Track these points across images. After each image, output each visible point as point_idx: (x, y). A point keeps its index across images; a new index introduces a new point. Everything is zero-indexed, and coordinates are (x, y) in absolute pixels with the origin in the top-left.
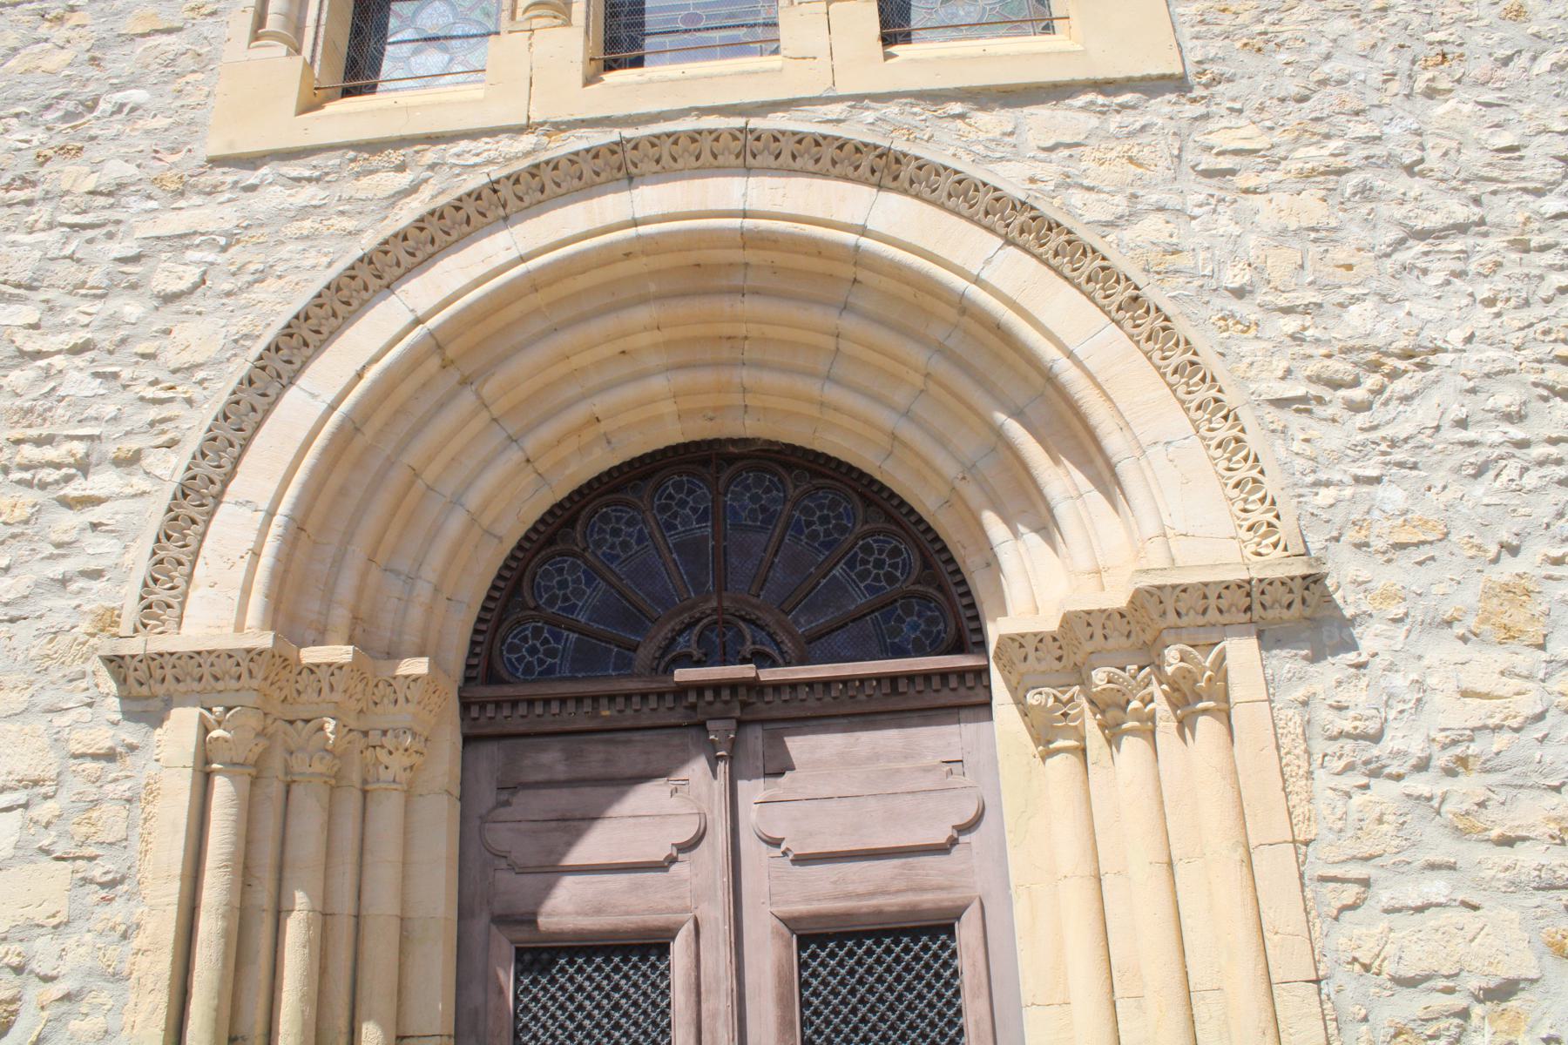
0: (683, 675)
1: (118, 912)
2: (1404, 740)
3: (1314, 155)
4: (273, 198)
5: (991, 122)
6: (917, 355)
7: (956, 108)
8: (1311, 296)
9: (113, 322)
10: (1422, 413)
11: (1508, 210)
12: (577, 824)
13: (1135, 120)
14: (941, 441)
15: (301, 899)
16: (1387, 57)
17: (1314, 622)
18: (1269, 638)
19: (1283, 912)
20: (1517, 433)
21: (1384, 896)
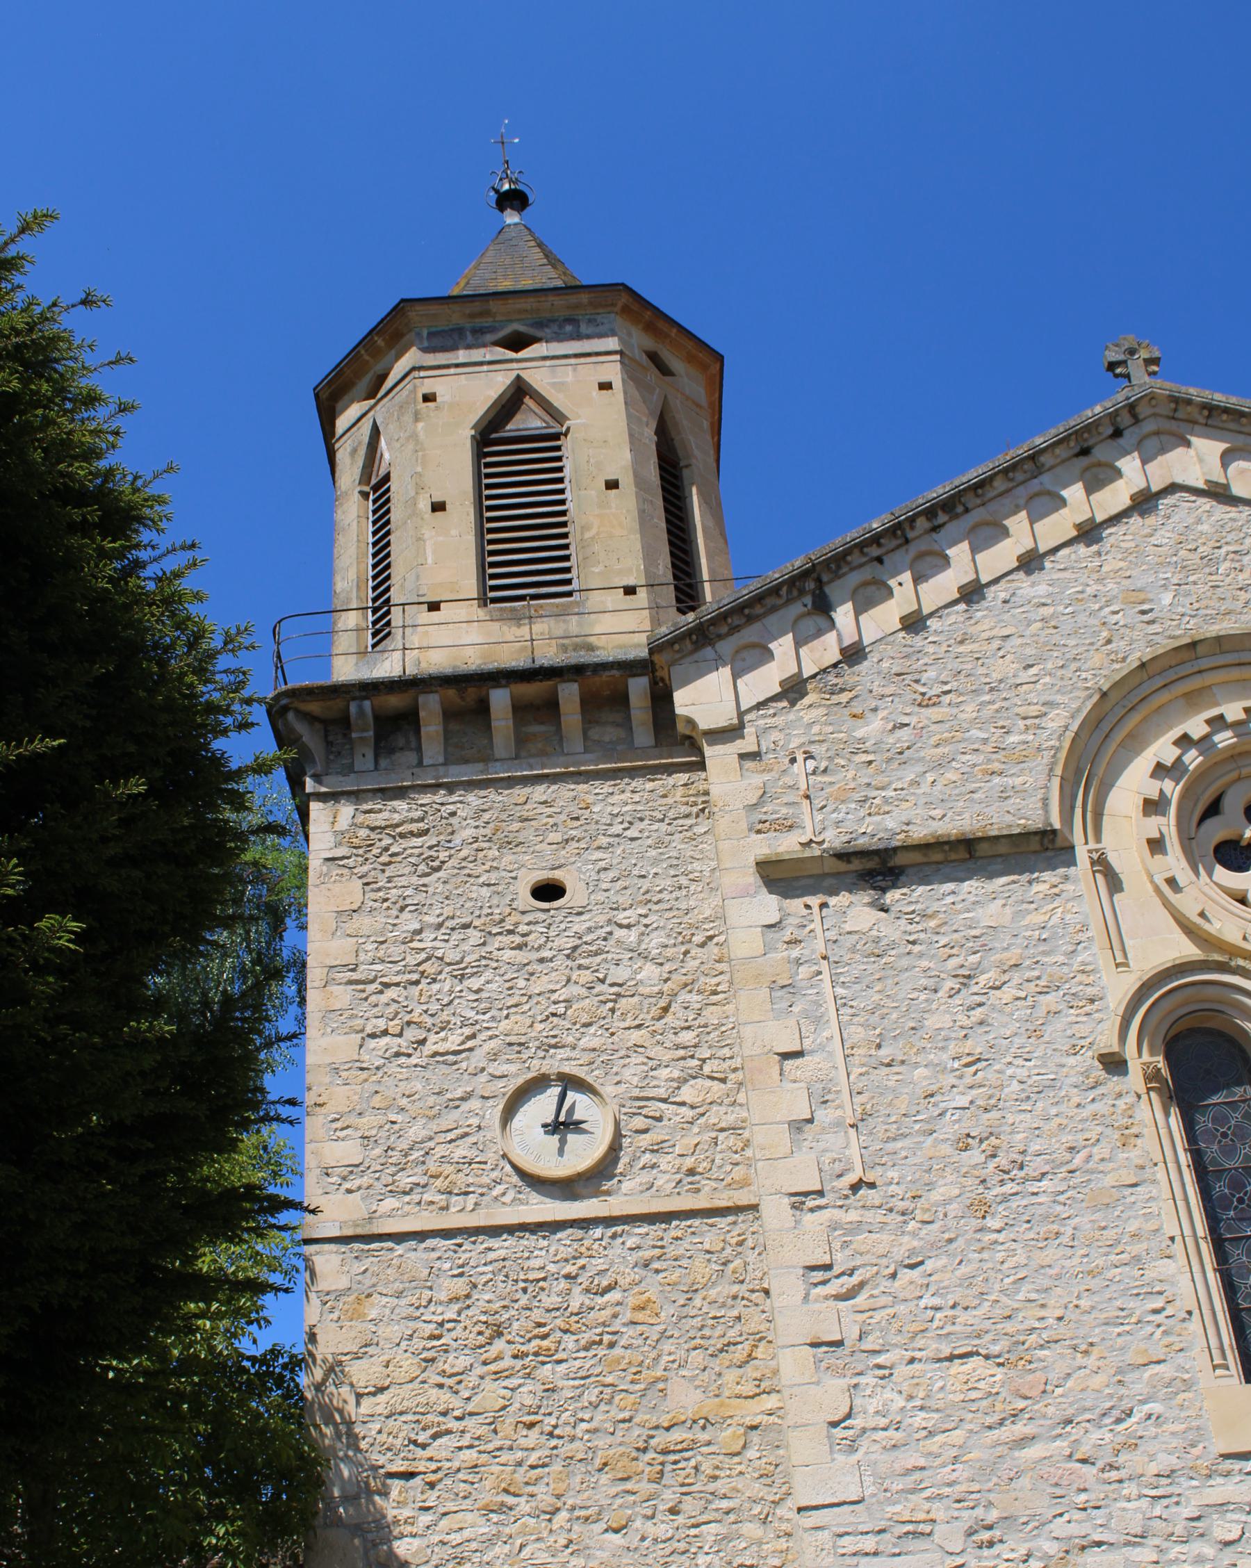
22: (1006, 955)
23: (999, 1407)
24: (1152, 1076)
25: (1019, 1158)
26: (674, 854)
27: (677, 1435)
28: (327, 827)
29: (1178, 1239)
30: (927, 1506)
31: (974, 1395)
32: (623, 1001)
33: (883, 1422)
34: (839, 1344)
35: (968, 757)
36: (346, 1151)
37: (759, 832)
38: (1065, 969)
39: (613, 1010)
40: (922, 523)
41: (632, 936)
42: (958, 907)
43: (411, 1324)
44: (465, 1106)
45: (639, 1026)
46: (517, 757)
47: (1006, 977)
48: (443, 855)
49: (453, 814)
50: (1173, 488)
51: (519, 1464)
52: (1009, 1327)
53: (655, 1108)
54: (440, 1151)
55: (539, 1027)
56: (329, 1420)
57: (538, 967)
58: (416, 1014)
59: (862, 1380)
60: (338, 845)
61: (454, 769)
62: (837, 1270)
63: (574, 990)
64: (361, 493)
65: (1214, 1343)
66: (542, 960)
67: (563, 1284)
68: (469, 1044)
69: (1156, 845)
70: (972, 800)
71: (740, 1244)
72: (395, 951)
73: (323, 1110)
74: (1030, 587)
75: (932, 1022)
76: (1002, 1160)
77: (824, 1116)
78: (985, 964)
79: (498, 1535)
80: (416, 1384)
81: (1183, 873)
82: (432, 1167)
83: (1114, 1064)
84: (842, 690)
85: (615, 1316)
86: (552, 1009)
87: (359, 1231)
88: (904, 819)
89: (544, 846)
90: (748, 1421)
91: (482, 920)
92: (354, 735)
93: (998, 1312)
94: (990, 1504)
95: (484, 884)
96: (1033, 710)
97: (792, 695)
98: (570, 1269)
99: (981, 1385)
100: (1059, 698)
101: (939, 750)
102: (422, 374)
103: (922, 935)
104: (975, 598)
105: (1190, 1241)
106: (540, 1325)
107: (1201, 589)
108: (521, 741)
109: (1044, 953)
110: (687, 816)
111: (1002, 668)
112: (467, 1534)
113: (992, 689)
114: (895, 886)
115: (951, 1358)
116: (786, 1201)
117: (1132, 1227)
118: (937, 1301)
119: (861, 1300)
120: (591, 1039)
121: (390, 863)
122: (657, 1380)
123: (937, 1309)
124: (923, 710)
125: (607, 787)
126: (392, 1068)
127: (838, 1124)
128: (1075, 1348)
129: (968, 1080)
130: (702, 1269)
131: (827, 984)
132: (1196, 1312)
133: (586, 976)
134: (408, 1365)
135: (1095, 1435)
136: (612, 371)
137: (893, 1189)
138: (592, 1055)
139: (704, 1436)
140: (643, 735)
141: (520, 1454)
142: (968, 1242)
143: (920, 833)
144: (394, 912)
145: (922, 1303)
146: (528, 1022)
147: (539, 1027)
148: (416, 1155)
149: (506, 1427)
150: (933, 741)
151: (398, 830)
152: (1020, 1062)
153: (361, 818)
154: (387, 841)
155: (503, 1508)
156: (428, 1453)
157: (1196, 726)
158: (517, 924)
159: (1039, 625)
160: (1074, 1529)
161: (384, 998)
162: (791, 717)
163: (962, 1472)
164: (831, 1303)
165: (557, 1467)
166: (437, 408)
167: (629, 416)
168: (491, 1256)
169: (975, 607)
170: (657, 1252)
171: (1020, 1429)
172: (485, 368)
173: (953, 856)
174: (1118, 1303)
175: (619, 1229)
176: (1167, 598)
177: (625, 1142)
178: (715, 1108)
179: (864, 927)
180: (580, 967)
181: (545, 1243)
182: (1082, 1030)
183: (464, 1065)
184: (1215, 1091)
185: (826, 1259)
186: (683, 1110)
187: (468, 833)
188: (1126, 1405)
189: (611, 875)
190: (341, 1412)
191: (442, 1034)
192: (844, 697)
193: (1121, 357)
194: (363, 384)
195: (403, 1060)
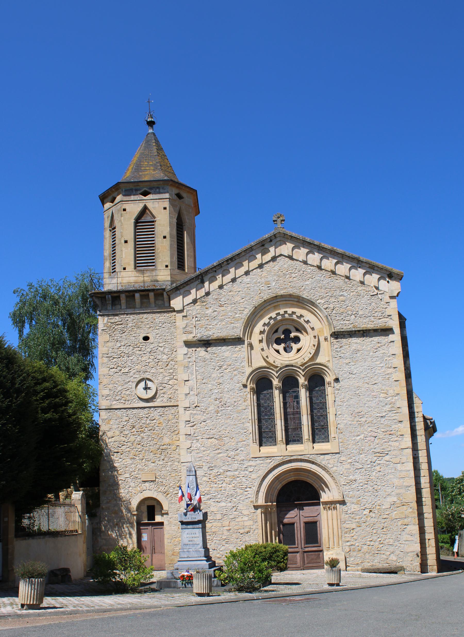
0: (295, 502)
1: (257, 524)
2: (349, 512)
3: (349, 461)
4: (258, 462)
5: (322, 456)
6: (315, 478)
7: (319, 455)
8: (347, 475)
9: (246, 474)
10: (354, 486)
11: (365, 467)
12: (286, 514)
13: (335, 457)
14: (317, 484)
15: (268, 522)
16: (358, 450)
17: (344, 503)
18: (340, 504)
19: (339, 524)
20: (362, 487)
21: (346, 523)
22: (229, 363)
23: (216, 447)
24: (252, 389)
25: (225, 403)
26: (171, 331)
27: (164, 447)
28: (102, 322)
29: (251, 420)
30: (202, 463)
31: (212, 445)
32: (159, 363)
33: (196, 449)
34: (190, 435)
35: (227, 319)
36: (106, 392)
37: (185, 334)
38: (239, 366)
39: (157, 365)
40: (225, 263)
42: (221, 352)
43: (118, 425)
44: (129, 384)
45: (162, 368)
46: (141, 308)
47: (228, 367)
48: (125, 330)
50: (281, 255)
51: (137, 451)
52: (219, 433)
53: (164, 385)
54: (124, 392)
55: (143, 368)
56: (103, 442)
58: (119, 364)
59: (194, 441)
60: (104, 326)
61: (128, 310)
62: (191, 422)
63: (151, 360)
64: (110, 230)
65: (254, 438)
66: (144, 354)
67: (146, 419)
68: (130, 371)
69: (261, 341)
70: (227, 329)
72: (116, 350)
73: (102, 383)
74: (246, 279)
75: (213, 376)
76: (222, 403)
77: (192, 393)
78: (224, 364)
79: (133, 463)
80: (119, 436)
82: (122, 396)
83: (245, 386)
84: (205, 302)
85: (155, 425)
86: (146, 364)
87: (109, 408)
88: (213, 332)
89: (145, 328)
90: (177, 445)
92: (107, 302)
93: (218, 431)
94: (212, 463)
96: (242, 309)
97: (194, 303)
98: (147, 416)
99: (213, 443)
100: (247, 307)
102: (123, 203)
103: (213, 358)
104: (234, 281)
105: (253, 420)
106: (141, 426)
107: (282, 282)
108: (142, 303)
111: (237, 299)
112: (128, 463)
113: (234, 304)
114: (210, 347)
115: (209, 438)
116: (183, 409)
117: (243, 417)
118: (208, 428)
119: (194, 427)
120: (153, 370)
121: (115, 331)
122: (162, 437)
123: (208, 430)
124: (220, 308)
125: (158, 315)
126: (115, 375)
127: (194, 394)
128: (230, 438)
129: (218, 387)
130: (171, 417)
132: (252, 433)
133: (152, 357)
134: (117, 433)
135: (231, 453)
136: (166, 204)
137: (202, 407)
138: (153, 374)
139: (169, 447)
141: (137, 449)
142: (214, 418)
143: (215, 336)
144: (116, 342)
145: (205, 428)
146: (141, 367)
147: (143, 368)
148: (119, 393)
149: (135, 444)
150: (221, 315)
151: (117, 323)
152: (228, 384)
153: (109, 320)
154: (114, 326)
155: (134, 458)
156: (121, 448)
157: (273, 315)
158: (140, 346)
159: (246, 289)
160: (226, 468)
161: (114, 361)
162: (194, 308)
163: (208, 458)
164: (190, 428)
165: (143, 452)
166: (126, 213)
167: (170, 217)
168: (133, 413)
169: (234, 283)
171: (219, 451)
172: (137, 202)
173: (221, 341)
174: (239, 430)
175: (156, 409)
176: (274, 284)
177: (158, 392)
178: (175, 386)
179: (203, 355)
180: (151, 355)
181: (142, 411)
183: (129, 375)
187: (130, 325)
188: (237, 448)
189: (159, 335)
190: (105, 440)
192: (205, 304)
193: (276, 219)
194: (110, 198)
195: (117, 374)
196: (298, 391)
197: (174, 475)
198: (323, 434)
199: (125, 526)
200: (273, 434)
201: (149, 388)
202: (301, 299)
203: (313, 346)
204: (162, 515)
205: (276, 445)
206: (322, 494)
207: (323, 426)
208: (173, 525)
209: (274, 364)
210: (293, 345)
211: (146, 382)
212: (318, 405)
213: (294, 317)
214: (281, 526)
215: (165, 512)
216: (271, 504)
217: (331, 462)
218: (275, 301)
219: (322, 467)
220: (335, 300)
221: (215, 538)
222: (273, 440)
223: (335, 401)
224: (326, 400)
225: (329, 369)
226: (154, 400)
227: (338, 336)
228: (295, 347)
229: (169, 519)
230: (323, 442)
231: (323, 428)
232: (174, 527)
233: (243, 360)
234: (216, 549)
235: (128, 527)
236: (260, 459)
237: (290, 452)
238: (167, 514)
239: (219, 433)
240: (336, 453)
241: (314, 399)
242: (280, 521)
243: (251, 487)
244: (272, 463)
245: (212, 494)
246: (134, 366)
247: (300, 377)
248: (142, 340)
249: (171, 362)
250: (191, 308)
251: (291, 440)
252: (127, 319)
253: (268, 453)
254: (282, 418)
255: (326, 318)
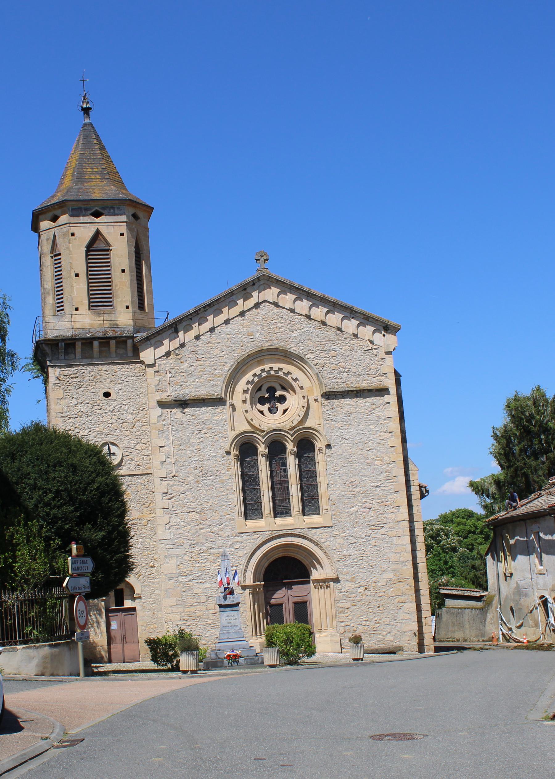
0: (283, 581)
1: (245, 606)
3: (343, 535)
4: (245, 538)
5: (314, 530)
6: (306, 554)
7: (310, 529)
8: (341, 550)
9: (231, 551)
10: (349, 562)
11: (360, 541)
12: (273, 594)
13: (327, 531)
14: (307, 560)
15: (256, 603)
16: (351, 523)
20: (356, 563)
24: (236, 456)
25: (206, 472)
28: (53, 375)
31: (193, 519)
32: (124, 424)
33: (176, 524)
35: (206, 376)
38: (221, 430)
39: (122, 426)
40: (203, 309)
41: (126, 407)
45: (127, 430)
46: (99, 358)
49: (84, 373)
50: (265, 301)
52: (201, 507)
53: (131, 450)
57: (105, 414)
58: (77, 425)
59: (172, 516)
61: (84, 360)
62: (168, 494)
63: (114, 421)
64: (51, 256)
66: (106, 413)
68: (89, 433)
69: (244, 402)
70: (205, 387)
71: (148, 481)
74: (226, 329)
75: (192, 441)
76: (203, 472)
77: (168, 461)
78: (204, 428)
81: (249, 409)
83: (228, 453)
84: (179, 355)
86: (108, 425)
90: (148, 519)
91: (92, 402)
92: (60, 351)
94: (194, 540)
95: (92, 392)
100: (228, 361)
101: (200, 373)
102: (71, 225)
104: (213, 331)
107: (266, 333)
108: (100, 352)
109: (217, 426)
110: (140, 376)
111: (217, 351)
114: (187, 408)
115: (189, 512)
116: (159, 479)
118: (188, 501)
120: (117, 433)
123: (187, 502)
125: (120, 367)
127: (171, 462)
128: (213, 511)
129: (198, 454)
130: (140, 487)
131: (170, 430)
133: (116, 417)
135: (215, 528)
136: (124, 229)
139: (139, 522)
140: (130, 353)
144: (71, 399)
145: (185, 501)
150: (199, 370)
151: (71, 376)
152: (209, 451)
154: (68, 379)
158: (100, 403)
159: (227, 340)
160: (209, 545)
162: (167, 361)
163: (189, 534)
164: (167, 500)
166: (75, 239)
167: (128, 245)
169: (213, 333)
170: (131, 483)
171: (201, 526)
172: (88, 225)
176: (257, 335)
180: (114, 415)
182: (223, 444)
184: (249, 457)
185: (167, 492)
186: (137, 451)
187: (88, 378)
188: (221, 523)
189: (122, 391)
191: (83, 431)
192: (179, 357)
193: (259, 258)
194: (50, 215)
196: (286, 458)
197: (146, 554)
198: (313, 506)
199: (91, 613)
200: (258, 506)
201: (114, 454)
202: (288, 353)
203: (302, 408)
204: (134, 599)
205: (262, 518)
206: (314, 571)
207: (313, 496)
208: (147, 611)
209: (259, 428)
210: (278, 405)
211: (109, 447)
212: (307, 474)
213: (281, 374)
214: (268, 607)
215: (138, 596)
216: (259, 583)
217: (323, 536)
218: (259, 355)
219: (314, 542)
220: (326, 355)
221: (199, 623)
222: (259, 513)
223: (326, 469)
224: (315, 468)
225: (320, 433)
226: (120, 468)
227: (330, 397)
228: (281, 407)
229: (142, 603)
230: (313, 514)
231: (313, 499)
232: (148, 613)
233: (225, 423)
234: (201, 634)
235: (95, 615)
236: (247, 534)
237: (279, 526)
238: (140, 598)
239: (201, 507)
240: (329, 527)
241: (303, 466)
242: (267, 603)
243: (237, 566)
244: (260, 539)
245: (195, 575)
246: (95, 427)
247: (288, 442)
248: (102, 397)
249: (137, 423)
250: (164, 362)
251: (278, 513)
252: (83, 371)
253: (255, 528)
254: (270, 489)
255: (316, 376)
